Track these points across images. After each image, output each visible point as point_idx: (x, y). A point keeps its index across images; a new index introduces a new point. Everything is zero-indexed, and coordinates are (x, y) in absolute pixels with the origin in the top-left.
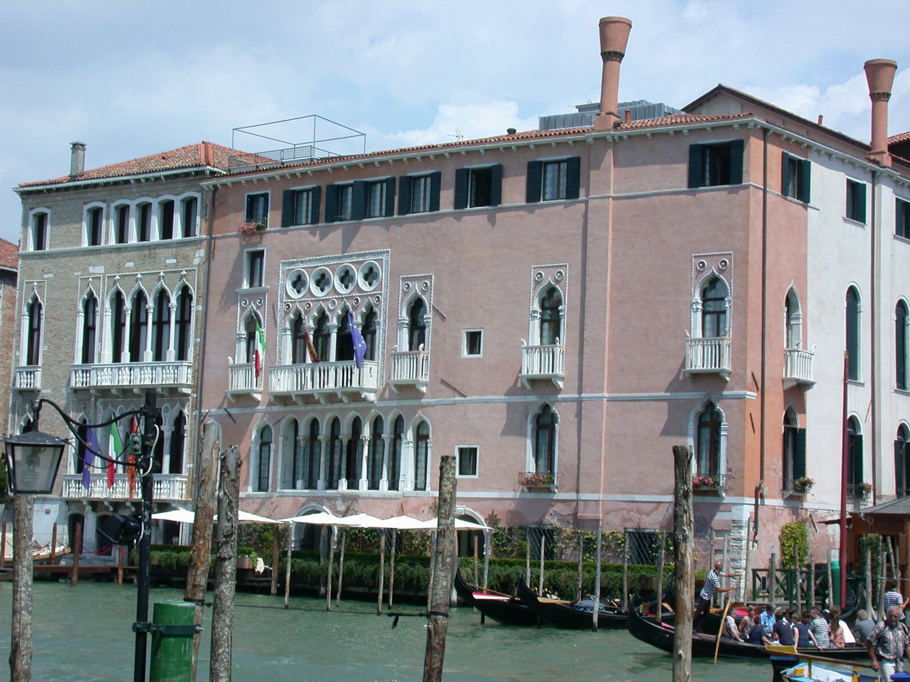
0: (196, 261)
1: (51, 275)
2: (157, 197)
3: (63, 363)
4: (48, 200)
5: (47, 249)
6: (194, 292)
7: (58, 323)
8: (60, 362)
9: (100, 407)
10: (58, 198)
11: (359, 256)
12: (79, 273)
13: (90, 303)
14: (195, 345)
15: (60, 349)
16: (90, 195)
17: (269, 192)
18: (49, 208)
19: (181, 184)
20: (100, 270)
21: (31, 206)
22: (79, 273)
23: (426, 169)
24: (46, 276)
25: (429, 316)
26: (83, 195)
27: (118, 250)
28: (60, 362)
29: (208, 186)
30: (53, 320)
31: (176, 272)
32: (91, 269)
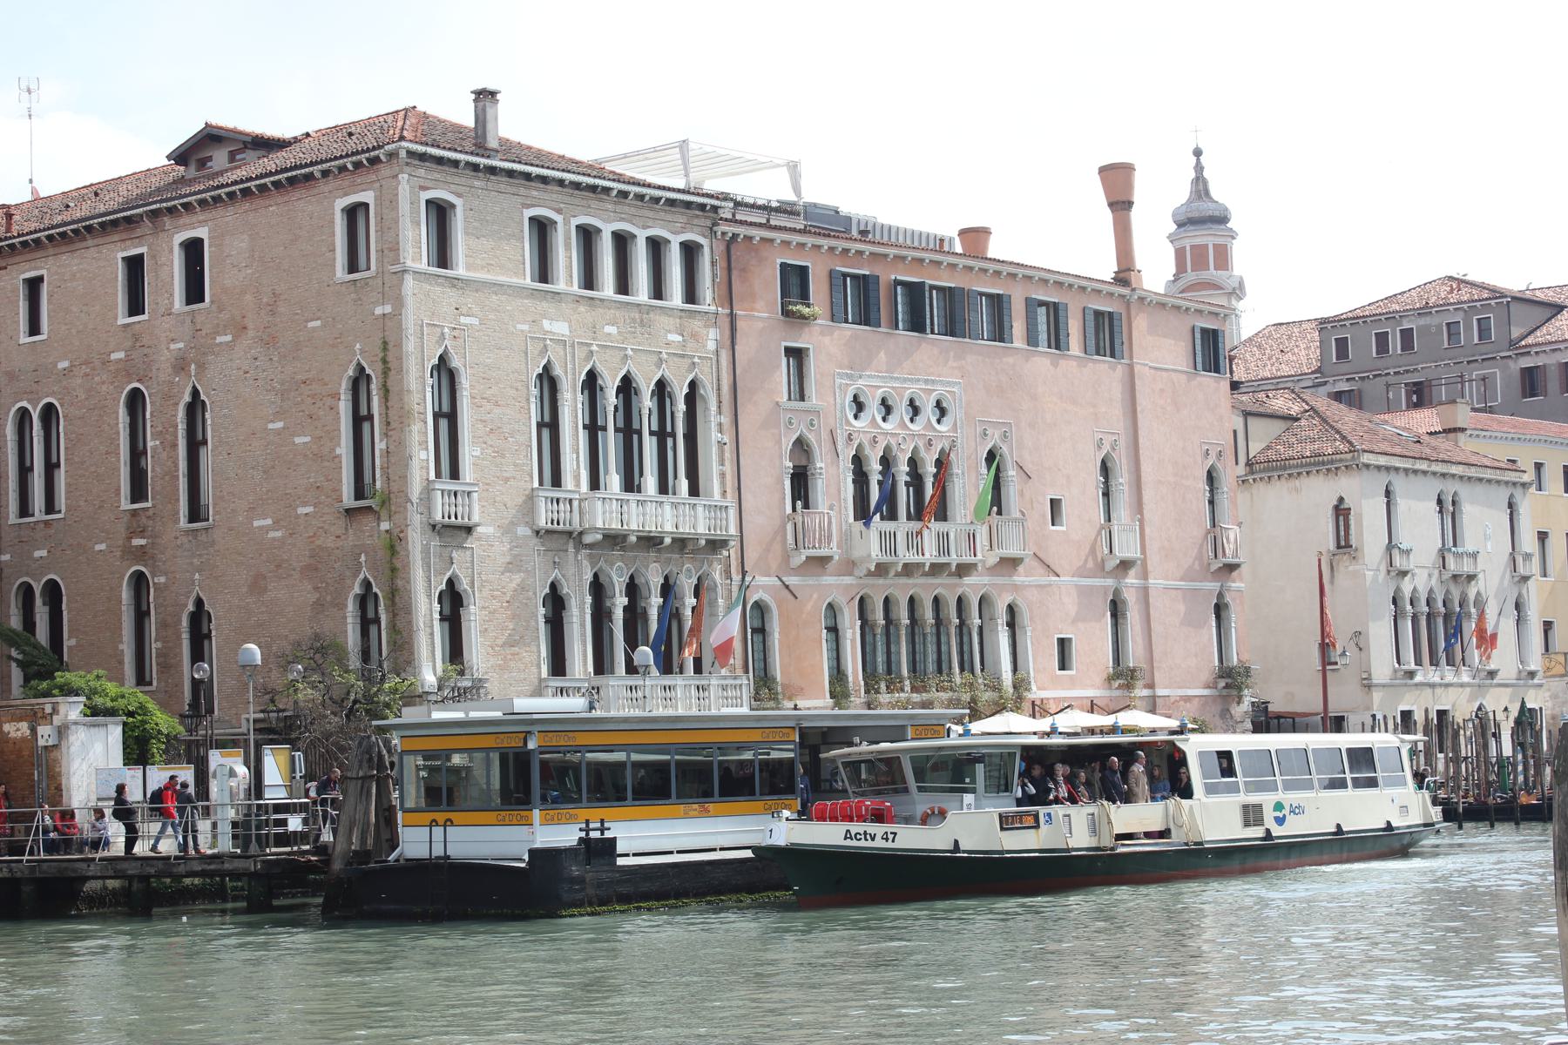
0: (711, 346)
1: (475, 321)
2: (645, 227)
3: (512, 482)
4: (457, 180)
5: (460, 270)
6: (708, 391)
7: (497, 411)
8: (507, 480)
9: (586, 563)
10: (477, 183)
11: (926, 382)
12: (525, 327)
13: (549, 382)
14: (723, 475)
15: (503, 456)
16: (535, 193)
17: (779, 261)
18: (459, 195)
19: (680, 218)
20: (561, 328)
21: (422, 182)
22: (525, 327)
23: (993, 286)
24: (463, 320)
25: (1011, 473)
26: (522, 191)
27: (578, 299)
28: (507, 480)
29: (724, 234)
30: (488, 406)
31: (683, 356)
32: (546, 324)
